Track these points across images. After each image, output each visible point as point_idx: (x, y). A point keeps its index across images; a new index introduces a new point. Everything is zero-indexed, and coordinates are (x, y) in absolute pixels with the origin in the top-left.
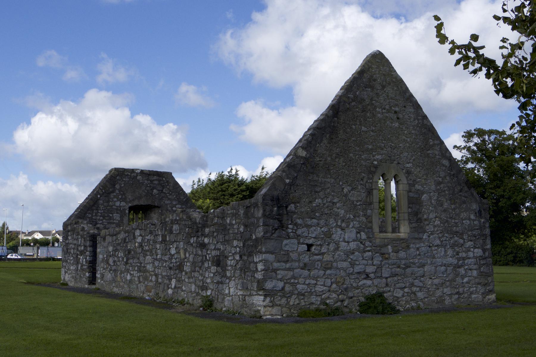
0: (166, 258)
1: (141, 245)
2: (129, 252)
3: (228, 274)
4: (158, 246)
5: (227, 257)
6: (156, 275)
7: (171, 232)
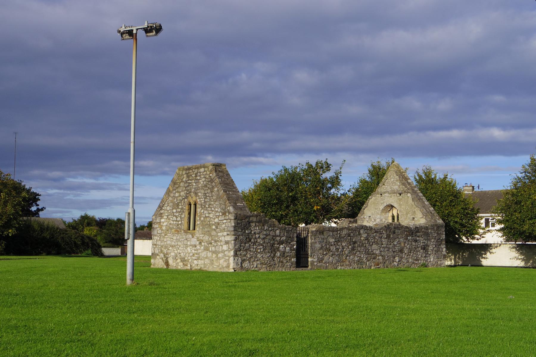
0: (391, 246)
1: (367, 239)
2: (355, 243)
3: (429, 253)
4: (383, 240)
5: (429, 246)
6: (382, 256)
7: (394, 233)
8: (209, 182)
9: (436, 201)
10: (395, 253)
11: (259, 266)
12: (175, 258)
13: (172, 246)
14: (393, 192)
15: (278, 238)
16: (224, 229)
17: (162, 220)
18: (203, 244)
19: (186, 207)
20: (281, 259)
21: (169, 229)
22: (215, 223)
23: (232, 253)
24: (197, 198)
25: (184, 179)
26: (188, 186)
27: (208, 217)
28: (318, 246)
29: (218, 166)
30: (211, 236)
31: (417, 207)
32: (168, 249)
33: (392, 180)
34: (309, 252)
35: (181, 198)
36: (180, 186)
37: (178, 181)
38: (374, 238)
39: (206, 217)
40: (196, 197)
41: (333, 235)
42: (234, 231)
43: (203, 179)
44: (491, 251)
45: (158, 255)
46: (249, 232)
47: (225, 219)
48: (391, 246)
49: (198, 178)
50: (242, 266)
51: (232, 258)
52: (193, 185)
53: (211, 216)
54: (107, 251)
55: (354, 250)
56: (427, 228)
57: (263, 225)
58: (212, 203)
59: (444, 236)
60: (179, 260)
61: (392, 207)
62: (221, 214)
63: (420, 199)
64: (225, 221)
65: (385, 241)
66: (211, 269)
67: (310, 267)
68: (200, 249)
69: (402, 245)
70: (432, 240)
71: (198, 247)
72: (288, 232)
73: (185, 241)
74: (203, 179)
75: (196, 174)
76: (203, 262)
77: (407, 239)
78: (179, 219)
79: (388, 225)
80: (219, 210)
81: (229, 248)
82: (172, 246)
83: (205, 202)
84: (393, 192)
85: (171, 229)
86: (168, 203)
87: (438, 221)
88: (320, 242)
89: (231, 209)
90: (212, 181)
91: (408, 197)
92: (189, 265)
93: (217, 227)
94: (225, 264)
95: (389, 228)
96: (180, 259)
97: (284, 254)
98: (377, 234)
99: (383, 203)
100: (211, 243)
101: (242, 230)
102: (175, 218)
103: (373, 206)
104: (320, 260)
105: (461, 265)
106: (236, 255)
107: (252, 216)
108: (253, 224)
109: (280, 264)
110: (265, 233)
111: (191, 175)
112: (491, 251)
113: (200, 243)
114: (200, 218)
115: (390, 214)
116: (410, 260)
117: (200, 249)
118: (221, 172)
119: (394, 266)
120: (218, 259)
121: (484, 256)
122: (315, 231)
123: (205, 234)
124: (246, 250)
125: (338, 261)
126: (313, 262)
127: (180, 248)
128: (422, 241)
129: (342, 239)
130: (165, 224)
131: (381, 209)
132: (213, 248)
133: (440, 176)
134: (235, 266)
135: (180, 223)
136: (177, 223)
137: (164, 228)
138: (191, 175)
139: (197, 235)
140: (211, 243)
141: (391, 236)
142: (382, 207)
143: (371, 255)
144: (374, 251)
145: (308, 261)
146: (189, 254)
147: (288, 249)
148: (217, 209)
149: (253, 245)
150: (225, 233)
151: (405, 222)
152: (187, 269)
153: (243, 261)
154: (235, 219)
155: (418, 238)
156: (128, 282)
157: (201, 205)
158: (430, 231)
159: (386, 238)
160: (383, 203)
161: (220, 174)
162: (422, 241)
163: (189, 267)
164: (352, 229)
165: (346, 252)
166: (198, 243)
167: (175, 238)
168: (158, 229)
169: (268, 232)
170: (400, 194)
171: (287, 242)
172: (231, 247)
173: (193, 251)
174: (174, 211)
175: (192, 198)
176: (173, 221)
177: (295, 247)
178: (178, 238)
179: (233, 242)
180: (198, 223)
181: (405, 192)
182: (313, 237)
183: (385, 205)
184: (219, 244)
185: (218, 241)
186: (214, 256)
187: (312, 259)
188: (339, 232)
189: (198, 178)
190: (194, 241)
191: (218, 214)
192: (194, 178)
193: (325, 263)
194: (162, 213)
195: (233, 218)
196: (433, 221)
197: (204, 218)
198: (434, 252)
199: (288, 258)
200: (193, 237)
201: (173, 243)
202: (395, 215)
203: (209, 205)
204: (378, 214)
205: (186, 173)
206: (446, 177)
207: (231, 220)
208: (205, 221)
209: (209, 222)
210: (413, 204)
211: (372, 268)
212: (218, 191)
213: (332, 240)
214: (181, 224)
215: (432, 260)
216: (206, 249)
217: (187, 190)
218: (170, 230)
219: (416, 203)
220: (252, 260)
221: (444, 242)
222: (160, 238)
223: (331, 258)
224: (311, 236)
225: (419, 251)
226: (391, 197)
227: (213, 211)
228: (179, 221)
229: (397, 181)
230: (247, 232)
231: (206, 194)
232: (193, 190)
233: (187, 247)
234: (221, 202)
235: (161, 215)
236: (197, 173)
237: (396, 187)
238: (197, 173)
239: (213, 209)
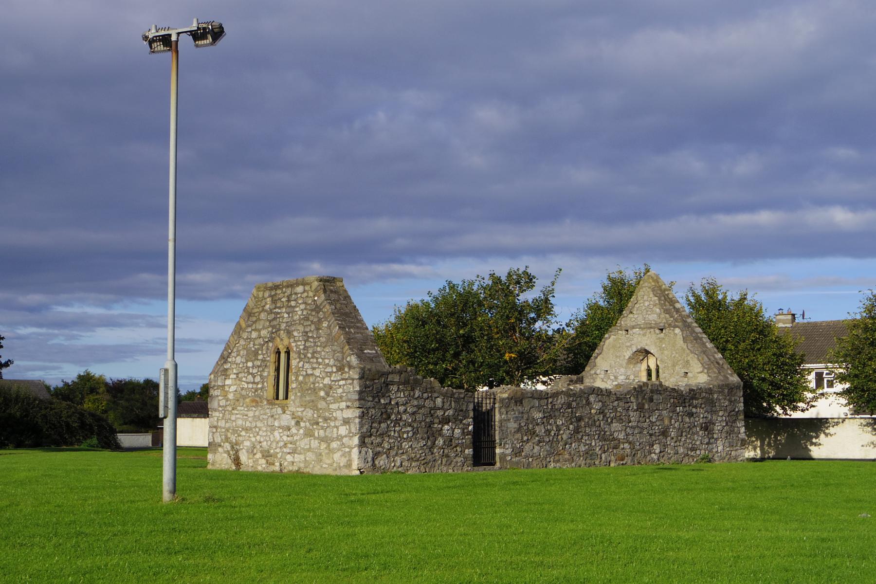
0: (645, 425)
1: (601, 412)
2: (580, 419)
3: (715, 436)
4: (631, 414)
5: (714, 424)
6: (630, 443)
7: (651, 400)
8: (312, 310)
9: (727, 341)
10: (654, 438)
11: (405, 464)
12: (252, 451)
13: (247, 430)
14: (649, 326)
15: (440, 413)
16: (341, 397)
17: (228, 382)
18: (302, 424)
19: (272, 358)
20: (446, 451)
21: (240, 398)
22: (325, 385)
23: (356, 440)
24: (292, 340)
26: (275, 319)
27: (312, 375)
28: (512, 425)
29: (328, 281)
30: (318, 410)
31: (692, 352)
32: (239, 436)
33: (647, 304)
34: (497, 438)
35: (261, 341)
36: (259, 319)
37: (256, 310)
38: (615, 409)
39: (307, 375)
40: (289, 338)
41: (540, 406)
42: (360, 399)
43: (302, 306)
44: (827, 431)
45: (220, 446)
46: (387, 401)
47: (343, 379)
48: (645, 425)
49: (293, 303)
50: (374, 465)
51: (355, 451)
53: (317, 373)
54: (126, 439)
55: (578, 433)
56: (710, 391)
57: (413, 390)
58: (319, 349)
59: (742, 404)
60: (259, 455)
61: (647, 353)
62: (335, 370)
63: (697, 338)
64: (342, 383)
65: (634, 416)
66: (317, 471)
67: (498, 465)
68: (296, 434)
69: (666, 422)
70: (721, 413)
71: (294, 430)
72: (457, 401)
73: (270, 419)
74: (302, 306)
75: (288, 297)
76: (302, 457)
77: (674, 411)
78: (258, 379)
79: (640, 387)
80: (332, 362)
81: (350, 432)
82: (247, 430)
83: (306, 348)
84: (649, 326)
85: (244, 397)
86: (238, 351)
87: (731, 378)
88: (516, 419)
89: (354, 360)
90: (317, 309)
92: (277, 464)
93: (328, 394)
94: (343, 461)
95: (642, 391)
96: (261, 452)
97: (451, 440)
98: (621, 404)
99: (630, 346)
100: (317, 423)
101: (374, 398)
102: (250, 378)
103: (611, 352)
104: (517, 452)
105: (773, 459)
106: (362, 444)
107: (392, 373)
108: (395, 388)
109: (444, 460)
110: (416, 403)
111: (280, 299)
112: (827, 431)
113: (298, 423)
115: (644, 366)
116: (681, 450)
118: (335, 292)
119: (652, 460)
120: (331, 451)
121: (814, 440)
122: (508, 398)
123: (305, 407)
124: (381, 435)
125: (550, 454)
126: (503, 456)
127: (261, 433)
128: (702, 414)
129: (557, 414)
130: (233, 388)
131: (627, 357)
132: (322, 432)
133: (733, 296)
134: (362, 465)
135: (260, 386)
136: (255, 386)
137: (231, 396)
138: (280, 299)
139: (292, 409)
140: (317, 423)
141: (646, 407)
142: (628, 354)
143: (610, 442)
144: (616, 434)
145: (494, 453)
146: (277, 443)
147: (457, 431)
148: (327, 361)
149: (394, 426)
150: (343, 405)
151: (671, 380)
152: (273, 472)
153: (376, 455)
154: (361, 378)
155: (694, 410)
156: (166, 496)
157: (299, 353)
158: (715, 396)
159: (637, 410)
160: (630, 346)
161: (333, 296)
162: (702, 414)
163: (277, 468)
164: (574, 394)
165: (565, 437)
166: (293, 423)
167: (251, 414)
168: (220, 398)
169: (421, 402)
170: (662, 330)
171: (455, 420)
172: (353, 430)
173: (285, 438)
174: (250, 364)
175: (282, 340)
176: (248, 383)
177: (471, 428)
178: (257, 413)
179: (357, 420)
180: (294, 385)
181: (670, 325)
182: (503, 410)
183: (635, 349)
184: (332, 424)
185: (330, 419)
186: (323, 446)
187: (502, 451)
188: (550, 400)
189: (293, 303)
190: (286, 419)
191: (329, 369)
192: (286, 304)
193: (527, 457)
194: (226, 370)
195: (357, 377)
196: (721, 378)
197: (304, 377)
198: (724, 435)
199: (459, 449)
200: (284, 412)
201: (248, 424)
202: (653, 367)
203: (314, 353)
204: (621, 366)
205: (270, 296)
206: (743, 298)
207: (353, 379)
208: (306, 383)
209: (314, 383)
210: (685, 347)
211: (612, 465)
212: (329, 327)
213: (538, 415)
214: (261, 389)
215: (720, 448)
216: (309, 434)
218: (241, 400)
219: (690, 345)
220: (393, 453)
221: (742, 417)
222: (224, 414)
223: (537, 448)
224: (500, 408)
225: (697, 433)
226: (644, 335)
227: (319, 364)
228: (257, 383)
229: (655, 305)
230: (382, 401)
231: (307, 333)
232: (283, 326)
233: (274, 430)
234: (335, 348)
235: (225, 373)
236: (291, 295)
237: (653, 317)
238: (291, 295)
239: (320, 360)
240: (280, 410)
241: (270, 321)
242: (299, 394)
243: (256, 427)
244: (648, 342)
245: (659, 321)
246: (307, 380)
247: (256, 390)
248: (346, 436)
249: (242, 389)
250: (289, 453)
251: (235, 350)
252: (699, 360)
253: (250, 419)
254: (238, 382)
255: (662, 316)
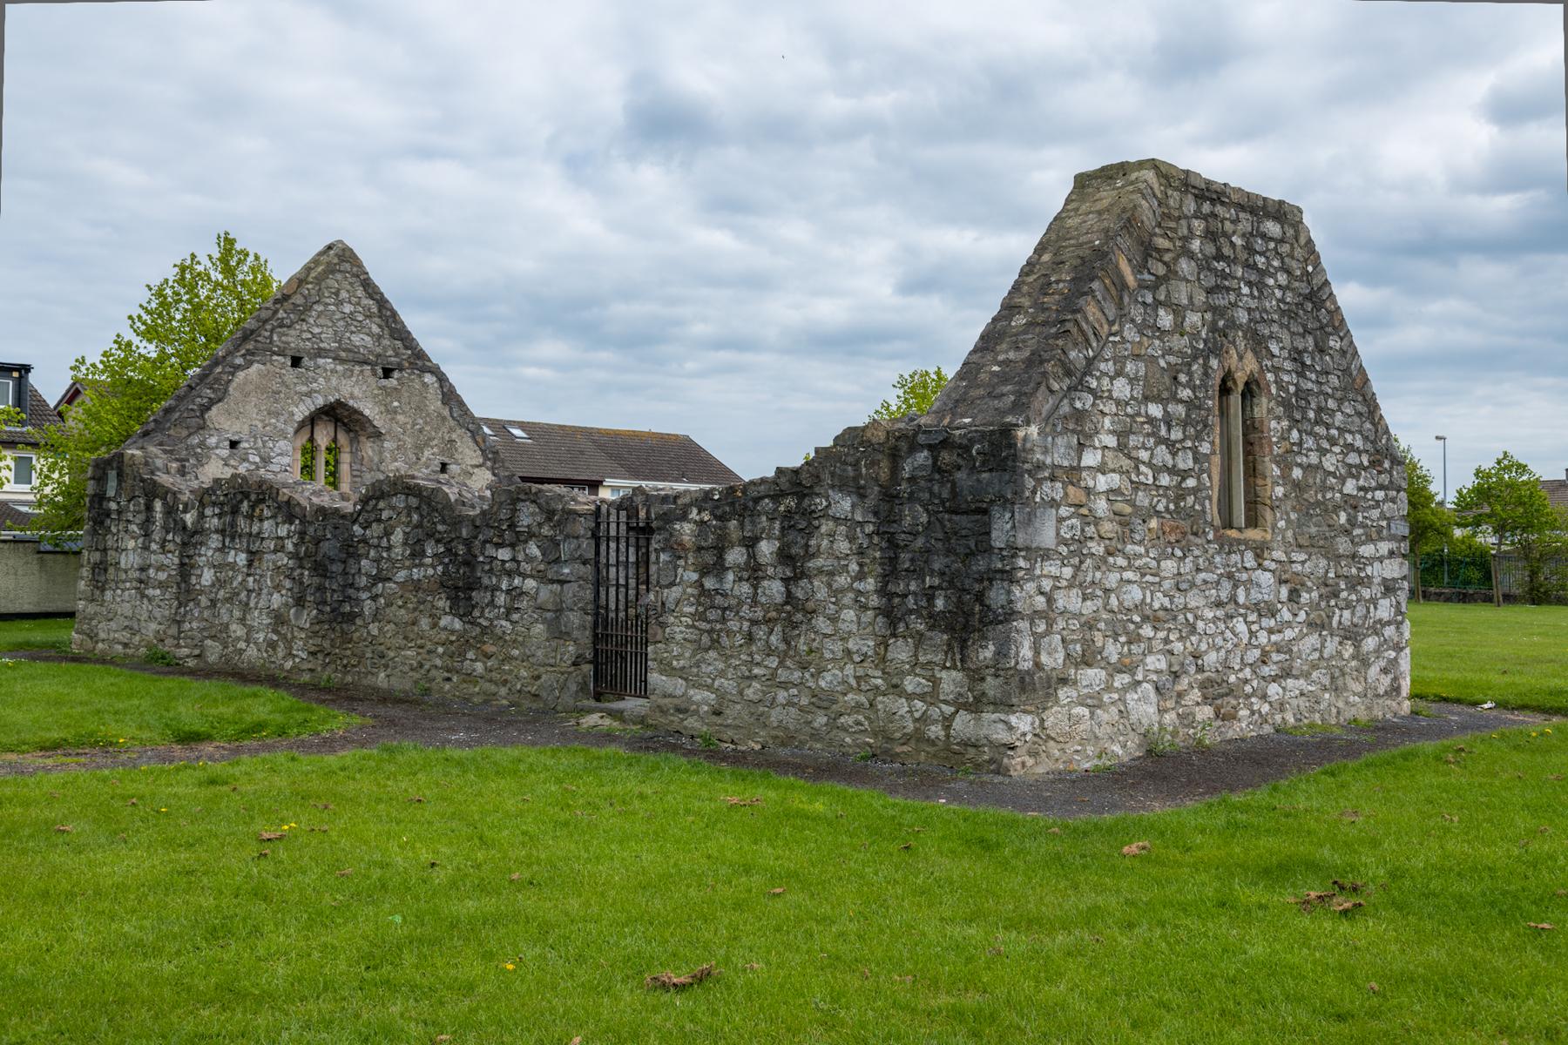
13: (1155, 620)
25: (1196, 245)
31: (461, 426)
33: (347, 308)
35: (1179, 343)
45: (1064, 681)
47: (1381, 487)
52: (1239, 295)
53: (1329, 463)
64: (1380, 495)
68: (1289, 624)
74: (1282, 278)
80: (1359, 443)
91: (425, 385)
93: (1352, 522)
94: (1386, 680)
99: (309, 394)
102: (1162, 453)
113: (1294, 595)
114: (1286, 467)
117: (1289, 624)
127: (1200, 624)
130: (1102, 482)
131: (299, 417)
135: (1191, 483)
137: (1101, 506)
142: (301, 411)
148: (1349, 438)
150: (1384, 547)
166: (1284, 592)
167: (1169, 566)
170: (387, 373)
173: (1263, 638)
174: (1155, 410)
181: (413, 366)
183: (320, 401)
184: (1366, 593)
191: (1353, 458)
201: (1160, 601)
203: (1319, 410)
210: (446, 412)
214: (1195, 491)
217: (1217, 311)
226: (348, 374)
228: (1184, 475)
231: (1300, 353)
237: (360, 340)
240: (1249, 560)
241: (1209, 291)
242: (1293, 516)
243: (1185, 607)
244: (356, 392)
245: (379, 350)
246: (1311, 481)
247: (1180, 497)
248: (1389, 623)
249: (1137, 486)
250: (1274, 679)
251: (1108, 354)
252: (476, 442)
253: (1167, 584)
254: (1126, 463)
255: (386, 342)
